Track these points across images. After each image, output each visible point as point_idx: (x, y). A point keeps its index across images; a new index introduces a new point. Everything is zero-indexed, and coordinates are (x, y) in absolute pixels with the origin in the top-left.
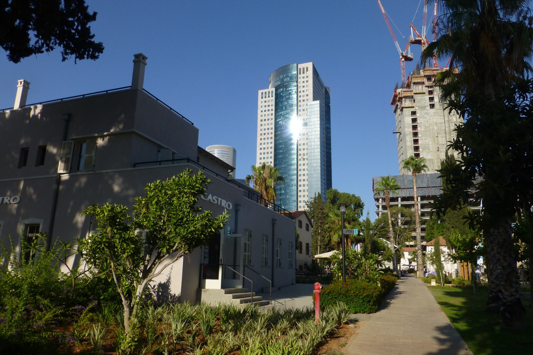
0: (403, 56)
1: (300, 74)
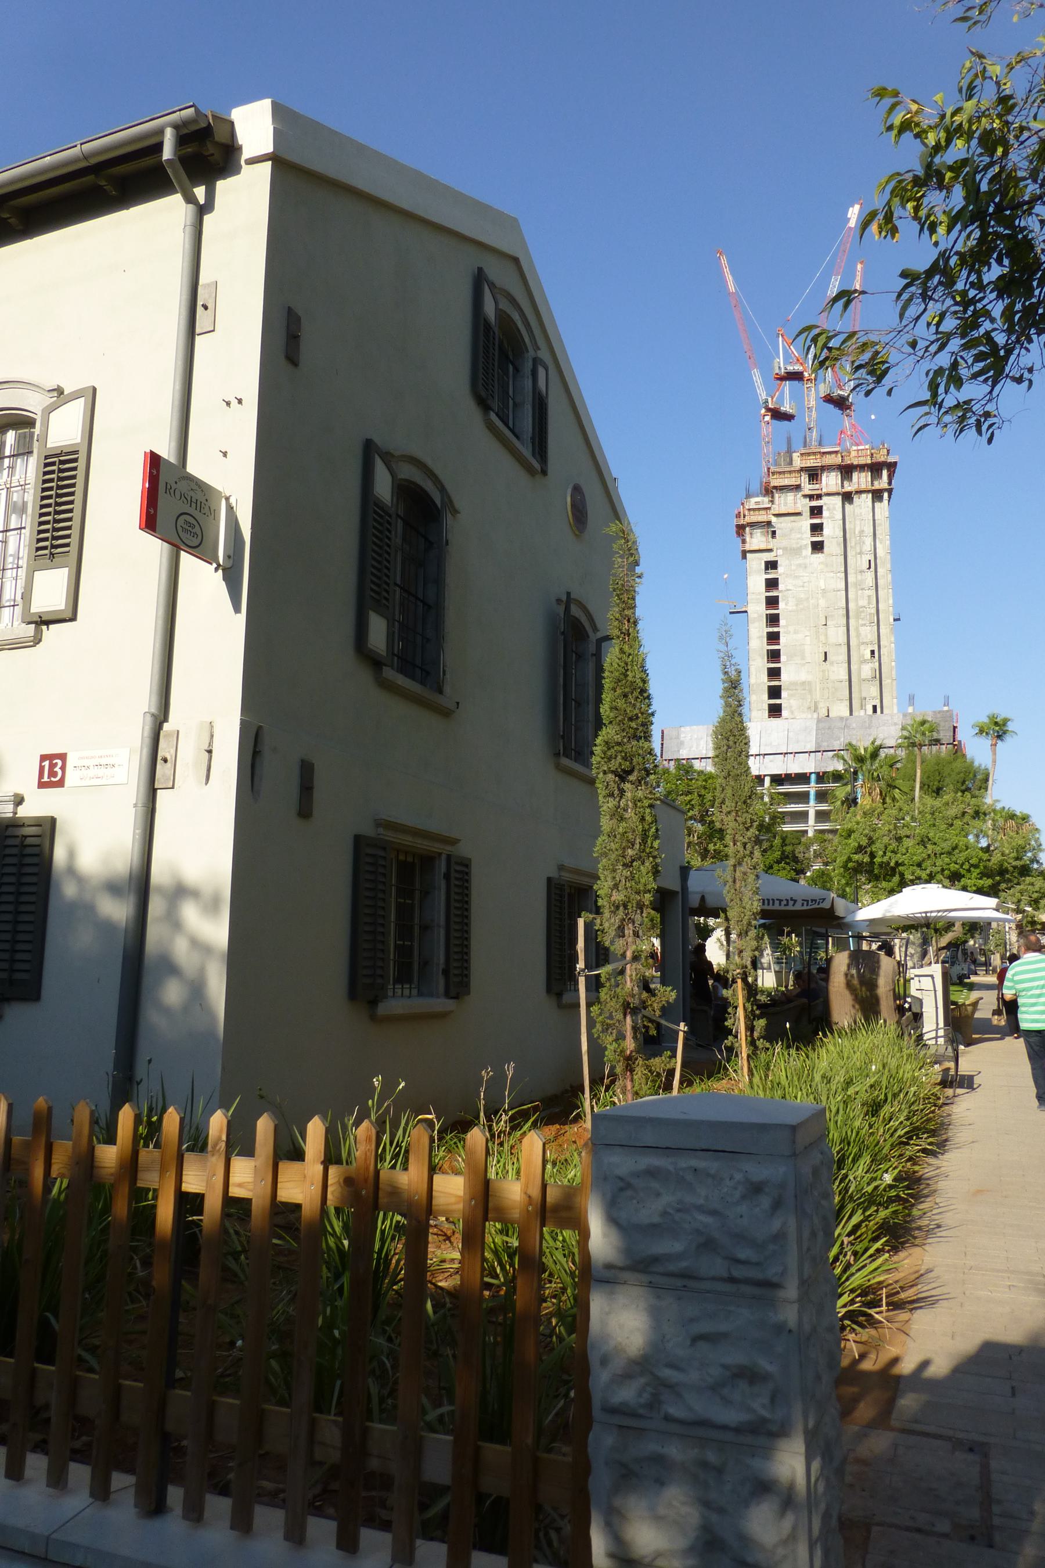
0: (768, 410)
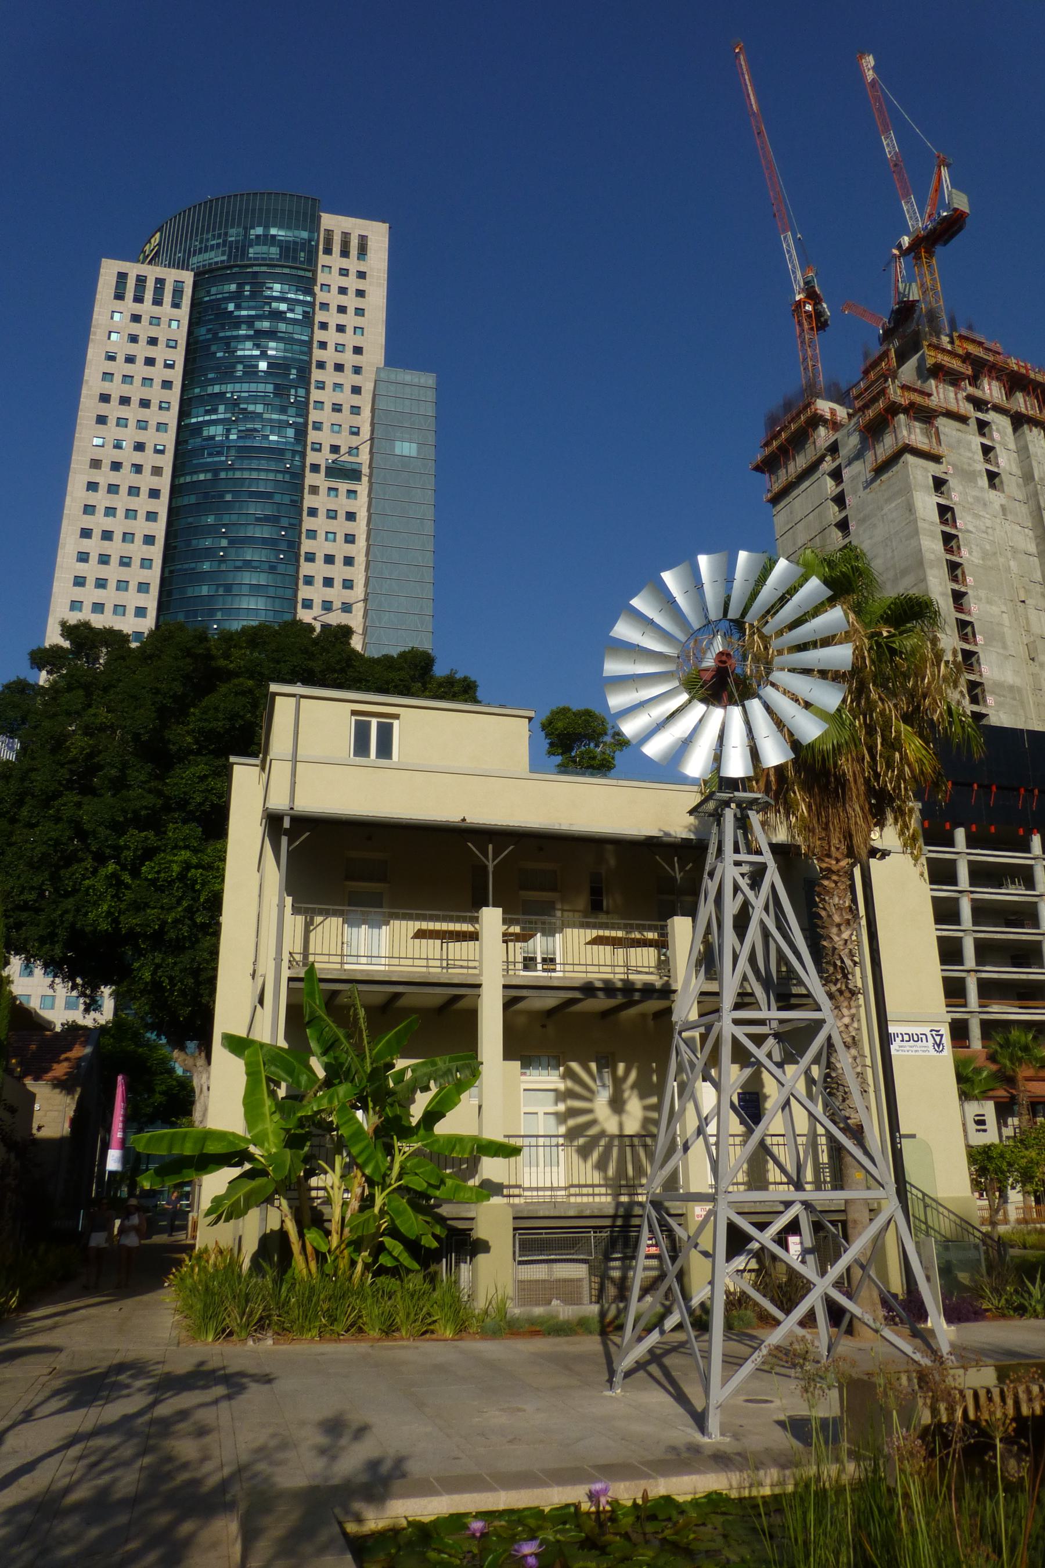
1: (328, 251)
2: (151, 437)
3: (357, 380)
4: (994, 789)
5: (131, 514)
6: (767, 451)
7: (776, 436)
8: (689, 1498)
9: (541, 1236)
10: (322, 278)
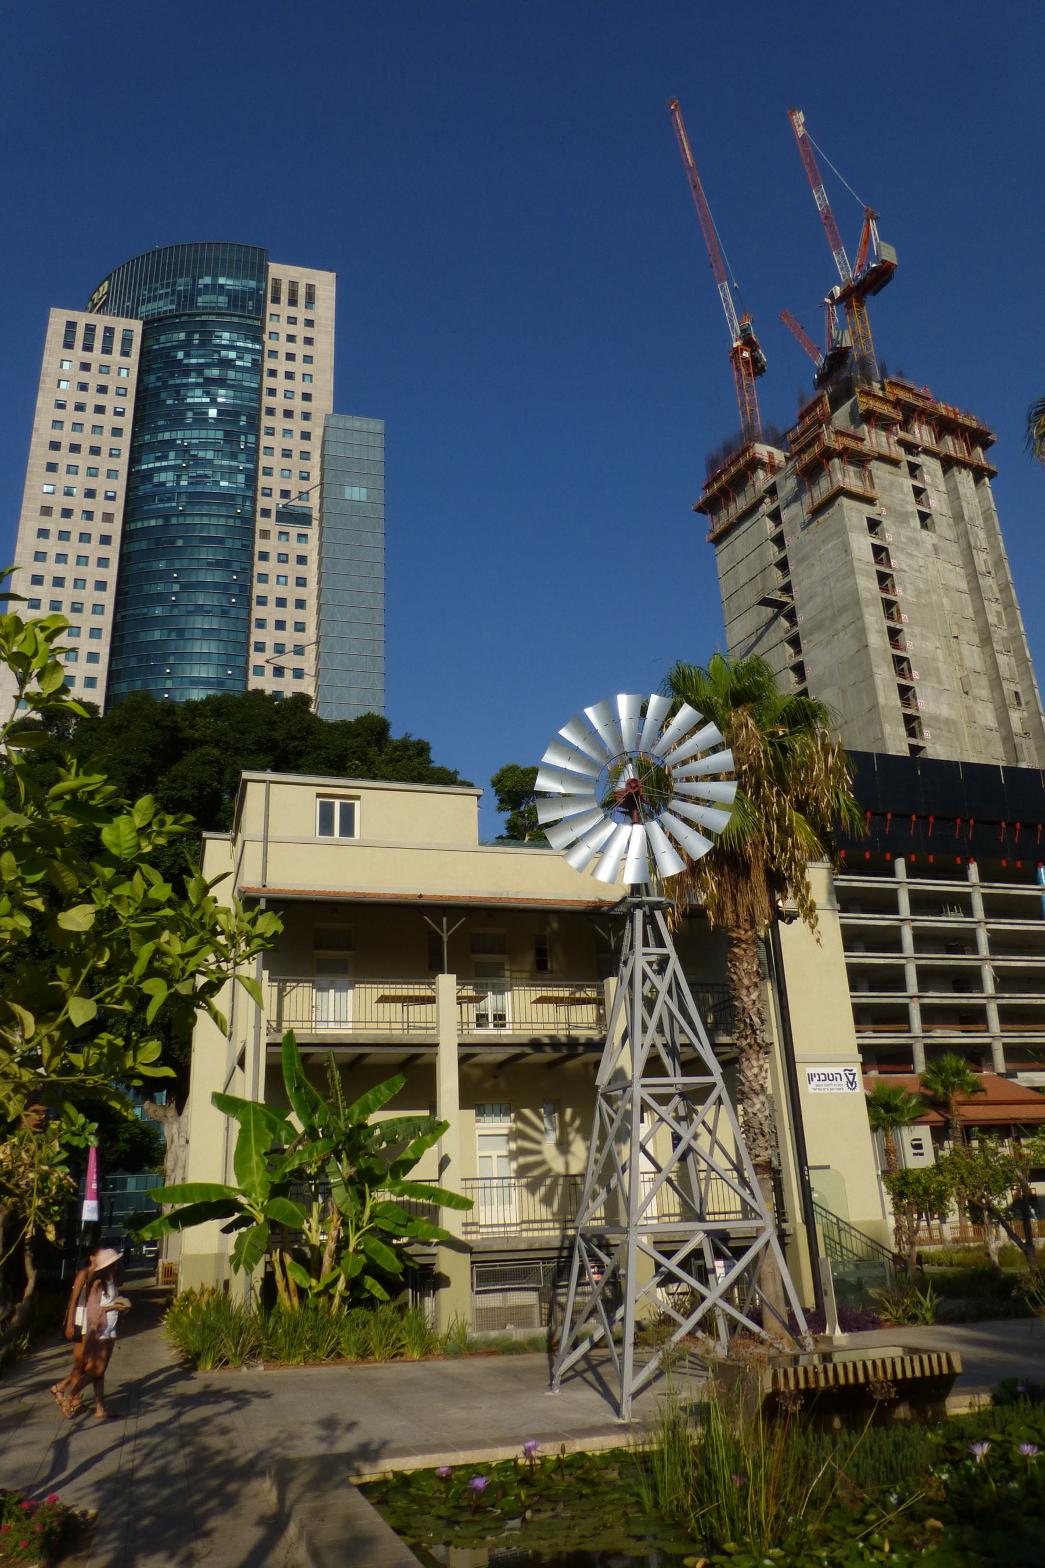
1: (276, 300)
2: (101, 484)
3: (306, 426)
4: (932, 820)
5: (82, 560)
6: (708, 493)
7: (716, 479)
8: (598, 1453)
9: (495, 1268)
10: (270, 326)
